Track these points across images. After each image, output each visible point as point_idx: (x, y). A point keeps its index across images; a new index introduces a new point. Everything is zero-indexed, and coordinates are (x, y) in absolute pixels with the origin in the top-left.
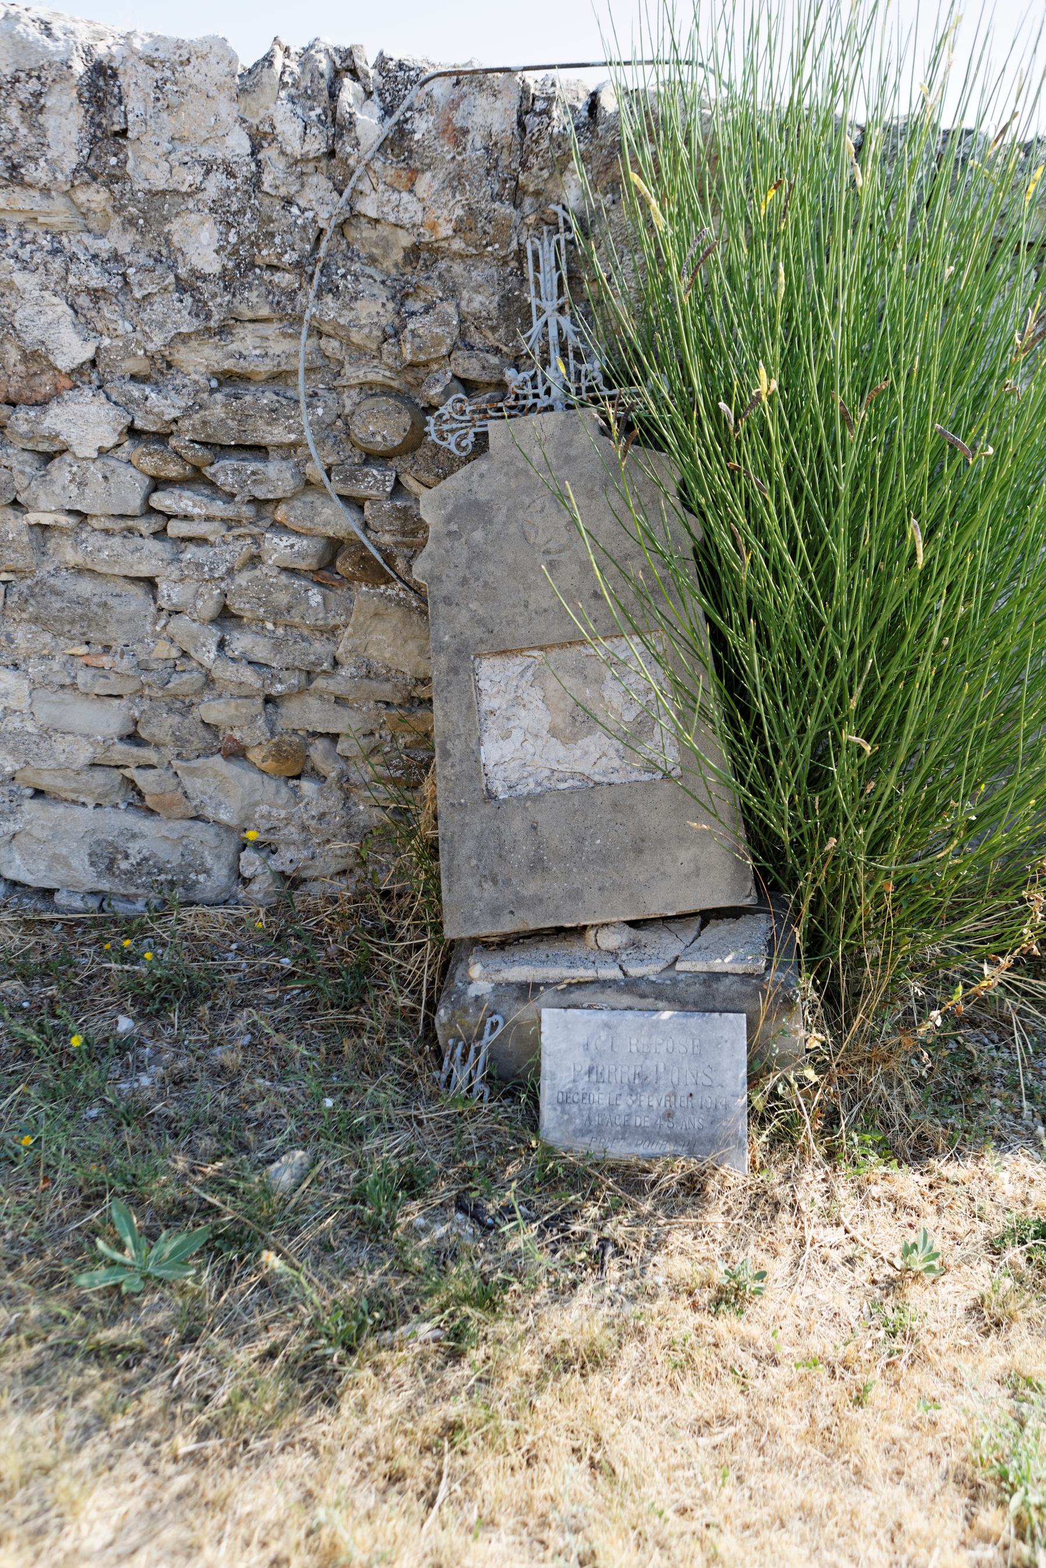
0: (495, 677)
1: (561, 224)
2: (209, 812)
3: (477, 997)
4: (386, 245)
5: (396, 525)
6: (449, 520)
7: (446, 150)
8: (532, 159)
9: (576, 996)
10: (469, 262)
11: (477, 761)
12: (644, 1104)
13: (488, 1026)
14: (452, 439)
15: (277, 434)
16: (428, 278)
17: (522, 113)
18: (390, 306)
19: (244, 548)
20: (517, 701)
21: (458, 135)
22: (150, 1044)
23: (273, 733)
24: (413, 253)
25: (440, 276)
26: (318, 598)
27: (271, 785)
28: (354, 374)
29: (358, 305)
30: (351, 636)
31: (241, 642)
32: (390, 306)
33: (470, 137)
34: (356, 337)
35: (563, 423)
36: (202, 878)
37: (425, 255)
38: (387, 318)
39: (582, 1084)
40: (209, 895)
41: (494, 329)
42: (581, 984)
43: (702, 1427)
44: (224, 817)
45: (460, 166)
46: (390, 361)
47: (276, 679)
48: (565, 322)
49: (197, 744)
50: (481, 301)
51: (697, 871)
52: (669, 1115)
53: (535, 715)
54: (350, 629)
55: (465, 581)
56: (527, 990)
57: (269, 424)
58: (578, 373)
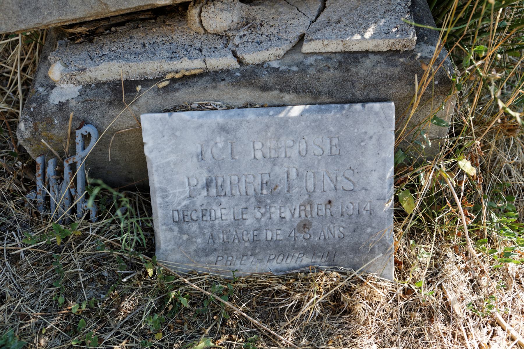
3: (61, 105)
9: (183, 95)
12: (276, 216)
13: (79, 139)
39: (201, 199)
42: (187, 79)
52: (305, 226)
56: (123, 91)
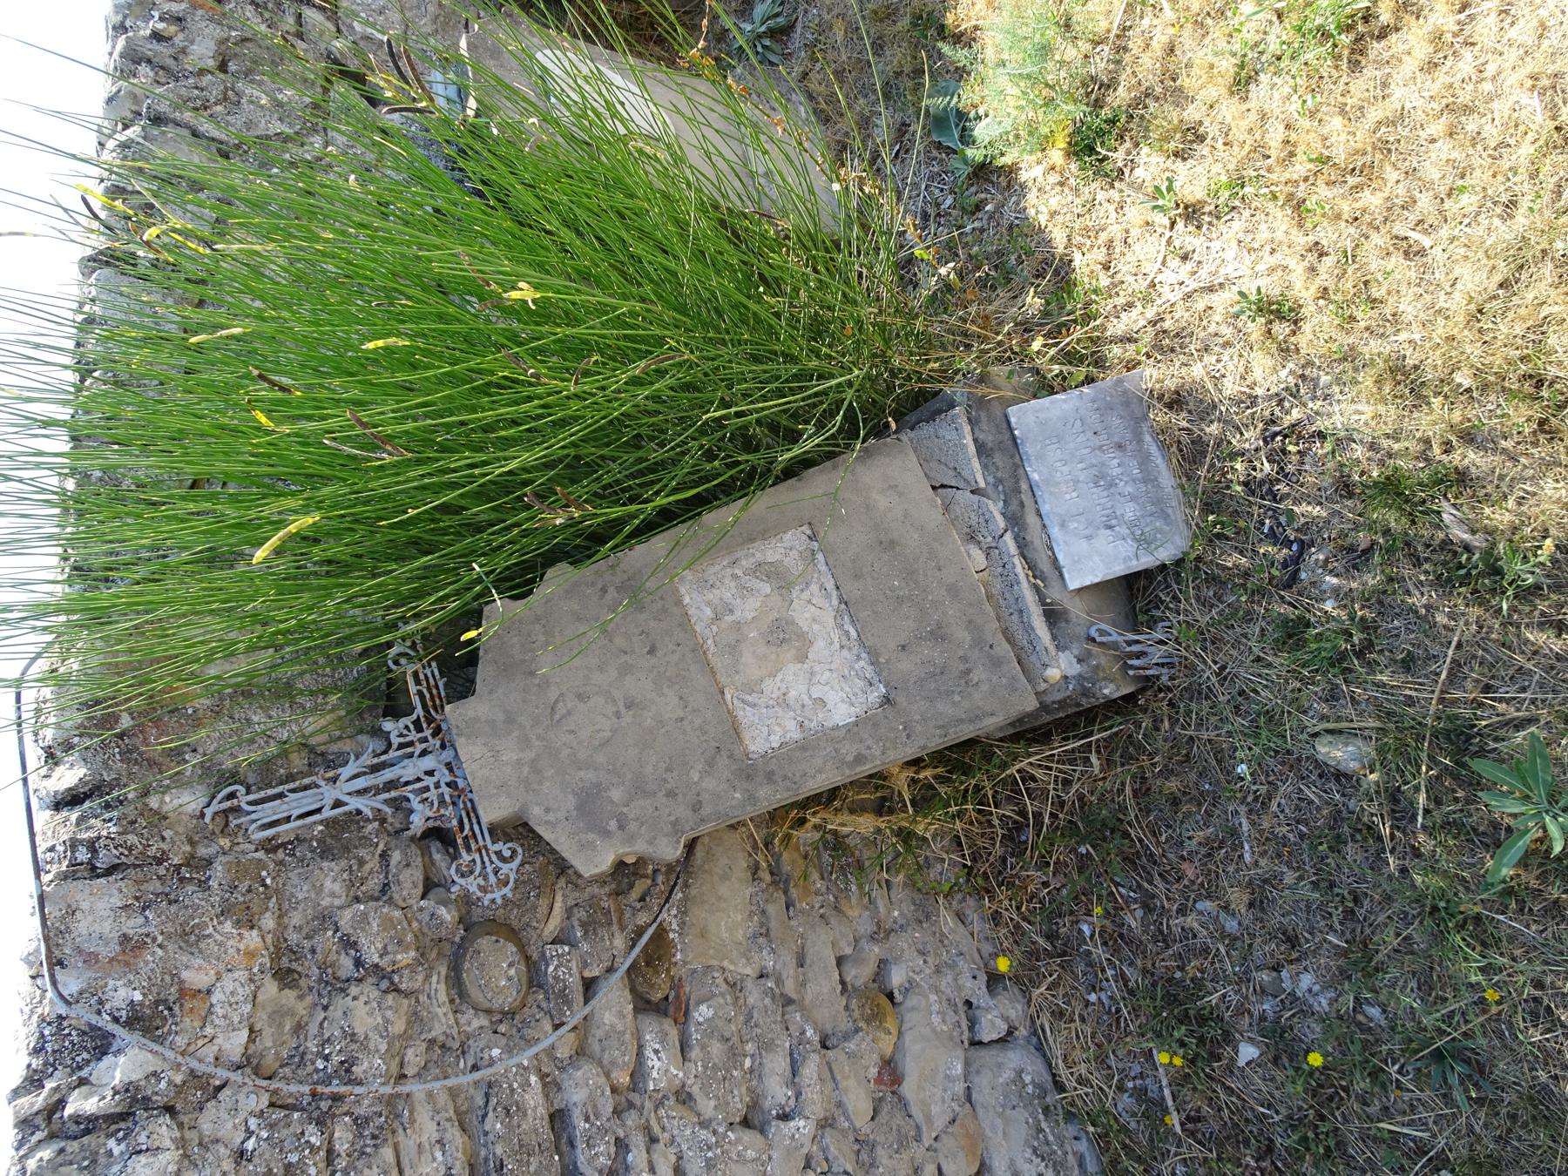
0: (766, 732)
1: (229, 804)
2: (959, 1088)
3: (1079, 661)
4: (278, 1014)
5: (602, 932)
6: (606, 833)
7: (151, 958)
8: (152, 851)
9: (1044, 565)
10: (286, 905)
11: (856, 724)
12: (1119, 470)
13: (1104, 639)
14: (505, 868)
15: (534, 1100)
16: (313, 951)
17: (93, 872)
18: (354, 990)
19: (672, 1109)
20: (783, 702)
21: (131, 946)
22: (1256, 1010)
23: (857, 1030)
24: (285, 977)
25: (308, 937)
26: (703, 1008)
27: (911, 1018)
28: (442, 1020)
29: (360, 1030)
30: (732, 962)
31: (777, 1092)
32: (354, 990)
33: (131, 932)
34: (399, 1027)
35: (469, 737)
36: (1028, 1079)
37: (285, 963)
38: (369, 991)
39: (1124, 531)
40: (1040, 1066)
41: (361, 862)
42: (1031, 566)
43: (1413, 253)
44: (959, 1068)
45: (169, 937)
46: (420, 978)
47: (802, 1040)
48: (346, 772)
49: (899, 1120)
50: (331, 881)
51: (893, 487)
52: (1120, 446)
53: (791, 680)
54: (726, 964)
55: (671, 794)
56: (1053, 616)
57: (525, 1114)
58: (401, 746)
